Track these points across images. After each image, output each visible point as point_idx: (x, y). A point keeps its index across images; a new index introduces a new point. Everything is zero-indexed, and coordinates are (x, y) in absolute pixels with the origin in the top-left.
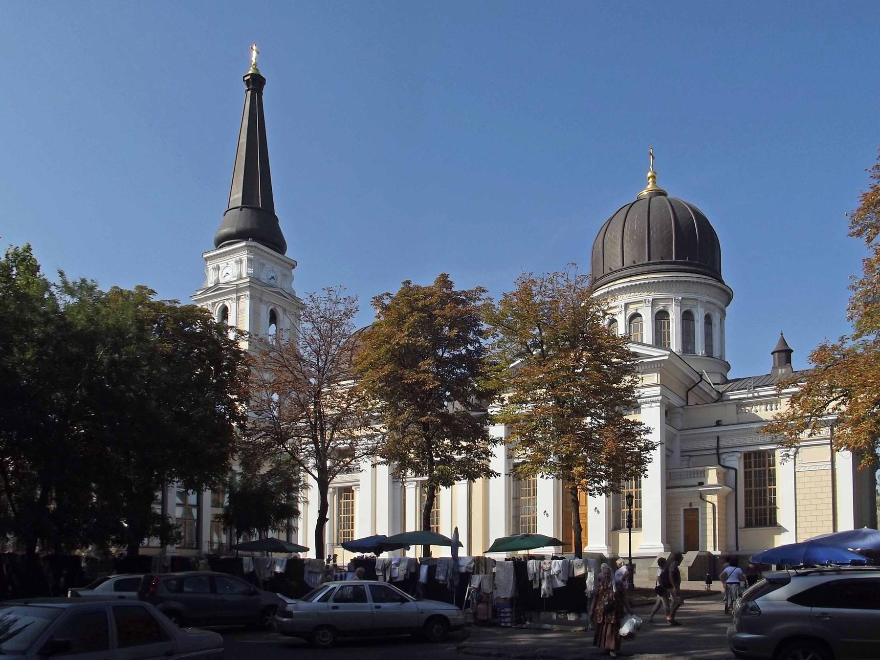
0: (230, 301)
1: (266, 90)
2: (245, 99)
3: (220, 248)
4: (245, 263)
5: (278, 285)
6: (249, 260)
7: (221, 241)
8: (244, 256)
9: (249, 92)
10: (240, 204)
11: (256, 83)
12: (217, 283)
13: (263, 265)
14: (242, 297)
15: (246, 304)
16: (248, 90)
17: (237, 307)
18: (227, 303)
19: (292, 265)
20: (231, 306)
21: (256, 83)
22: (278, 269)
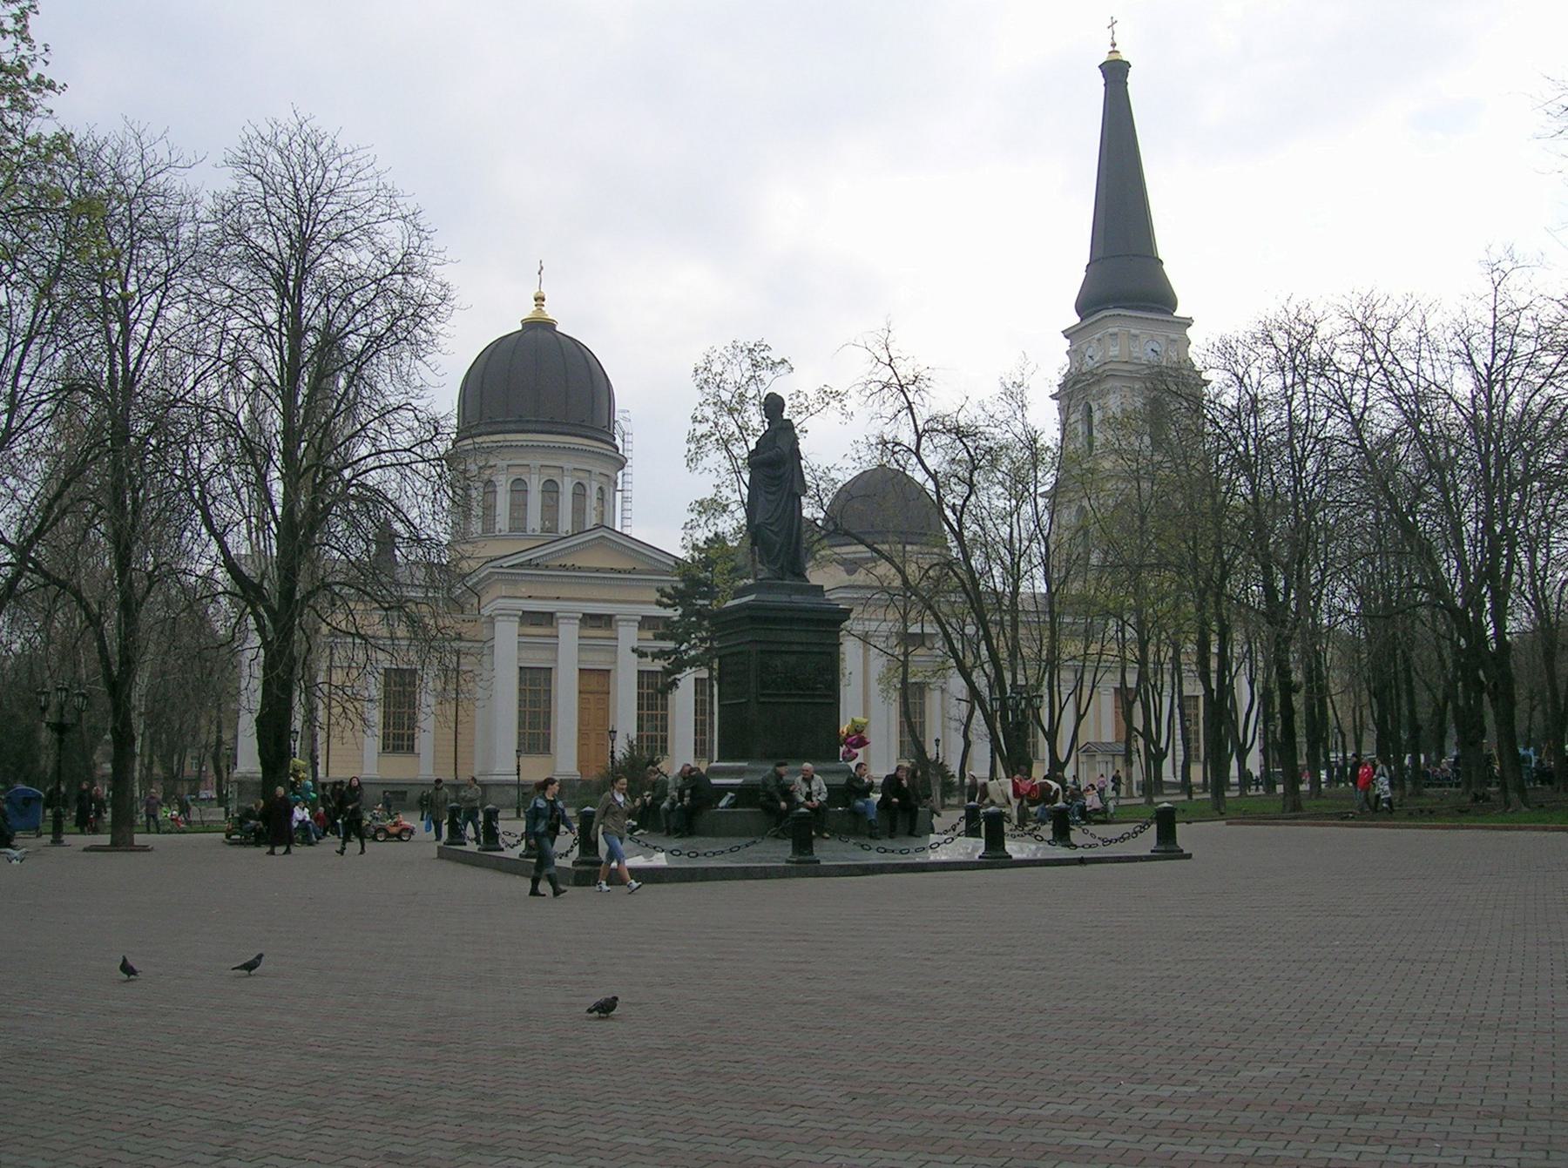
1: (1131, 79)
11: (1115, 72)
21: (1115, 72)
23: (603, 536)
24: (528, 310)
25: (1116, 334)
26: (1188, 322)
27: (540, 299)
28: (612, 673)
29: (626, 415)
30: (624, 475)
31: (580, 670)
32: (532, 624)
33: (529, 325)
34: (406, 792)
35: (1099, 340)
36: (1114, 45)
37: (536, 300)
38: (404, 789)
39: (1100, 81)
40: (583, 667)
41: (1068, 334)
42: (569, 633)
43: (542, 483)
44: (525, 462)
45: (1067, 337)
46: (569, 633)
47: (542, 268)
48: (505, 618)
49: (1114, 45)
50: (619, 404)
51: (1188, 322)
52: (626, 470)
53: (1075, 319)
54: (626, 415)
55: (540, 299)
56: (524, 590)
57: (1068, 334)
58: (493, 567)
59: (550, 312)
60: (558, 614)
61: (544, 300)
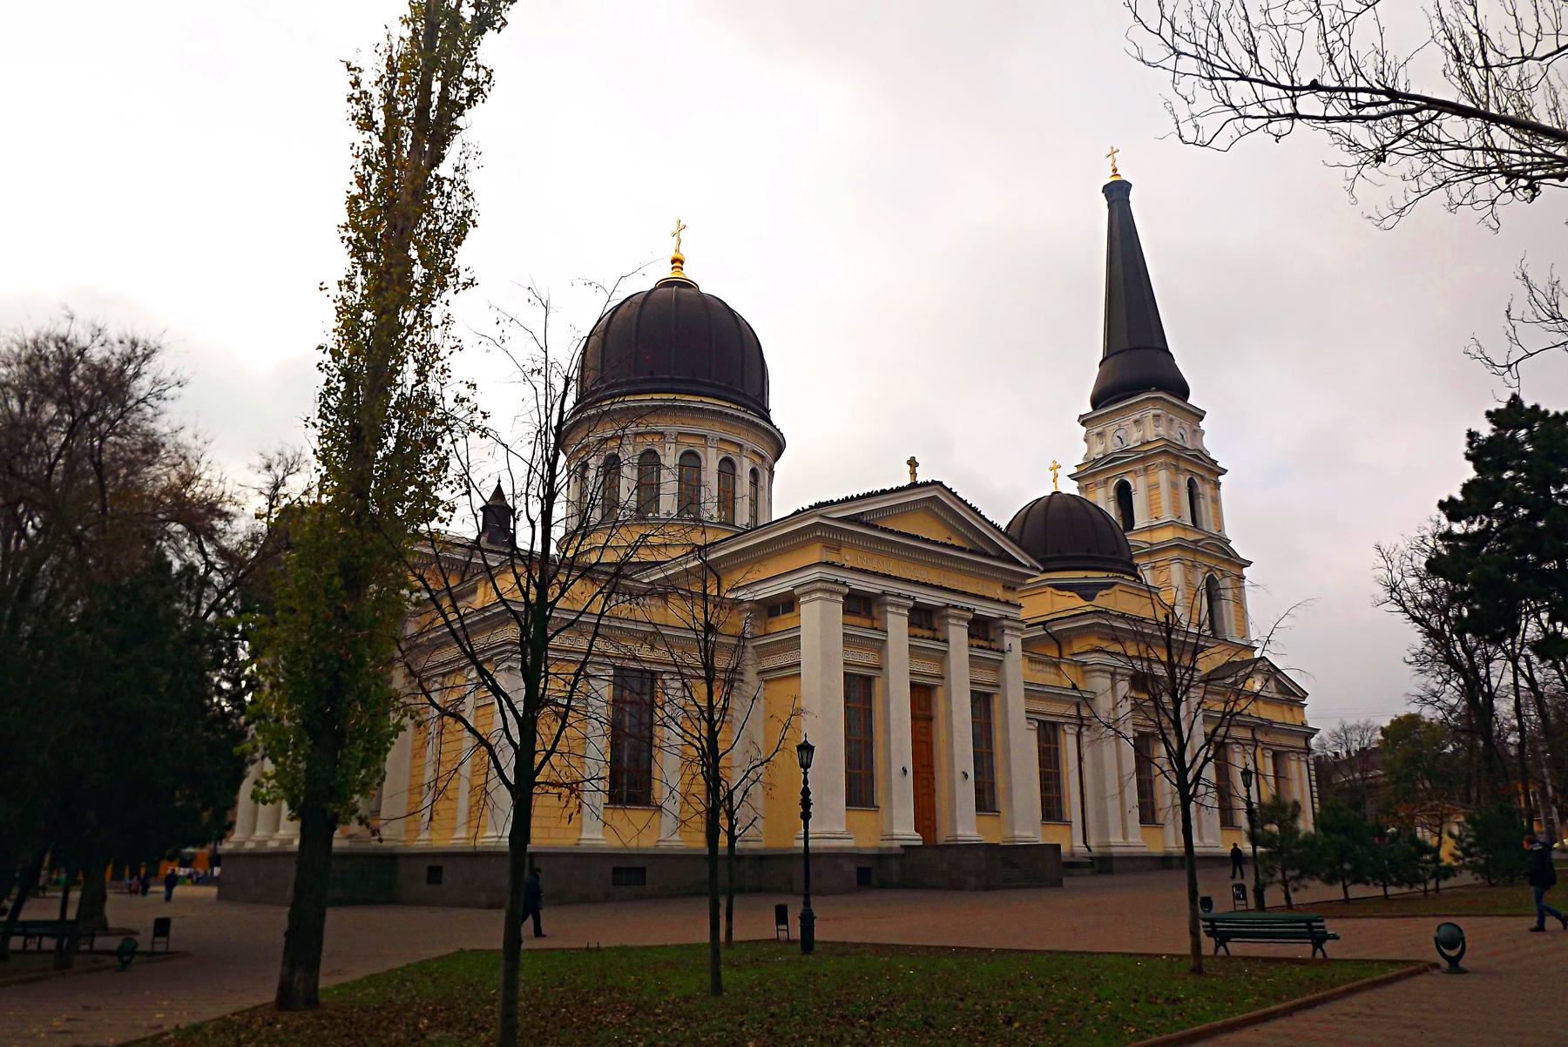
0: (1131, 474)
11: (1117, 193)
13: (1172, 420)
14: (1152, 467)
19: (1197, 415)
21: (1117, 193)
24: (666, 272)
25: (1158, 416)
26: (1199, 415)
27: (677, 262)
28: (940, 692)
33: (667, 283)
34: (643, 870)
35: (1136, 422)
36: (1115, 170)
37: (673, 261)
38: (639, 863)
39: (1103, 202)
40: (918, 680)
41: (1085, 421)
44: (700, 431)
45: (1083, 424)
48: (827, 596)
49: (1115, 170)
51: (1199, 415)
53: (1089, 409)
55: (677, 262)
56: (849, 558)
57: (1085, 421)
58: (822, 516)
59: (690, 272)
61: (682, 263)
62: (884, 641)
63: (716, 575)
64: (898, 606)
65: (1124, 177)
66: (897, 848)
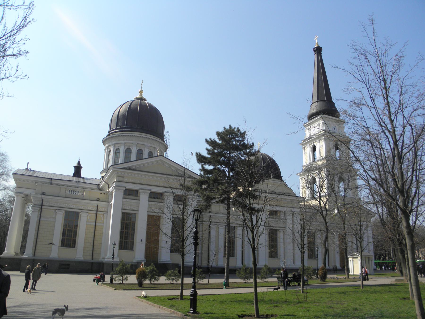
2: (313, 57)
3: (311, 120)
4: (321, 124)
5: (337, 132)
6: (322, 123)
7: (311, 117)
8: (321, 122)
9: (316, 55)
10: (317, 100)
11: (318, 50)
12: (310, 136)
15: (323, 143)
16: (315, 54)
17: (319, 145)
18: (315, 144)
20: (317, 144)
21: (318, 50)
22: (336, 125)
23: (161, 160)
27: (141, 92)
29: (168, 133)
30: (166, 153)
31: (148, 215)
32: (128, 195)
42: (144, 198)
43: (137, 150)
46: (144, 198)
47: (142, 84)
50: (166, 129)
52: (167, 152)
54: (168, 133)
55: (141, 92)
59: (144, 96)
60: (140, 191)
62: (139, 203)
63: (108, 184)
64: (145, 193)
65: (320, 46)
66: (134, 262)
